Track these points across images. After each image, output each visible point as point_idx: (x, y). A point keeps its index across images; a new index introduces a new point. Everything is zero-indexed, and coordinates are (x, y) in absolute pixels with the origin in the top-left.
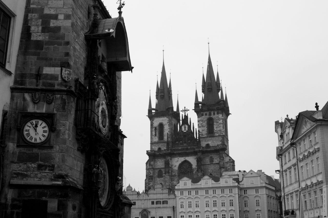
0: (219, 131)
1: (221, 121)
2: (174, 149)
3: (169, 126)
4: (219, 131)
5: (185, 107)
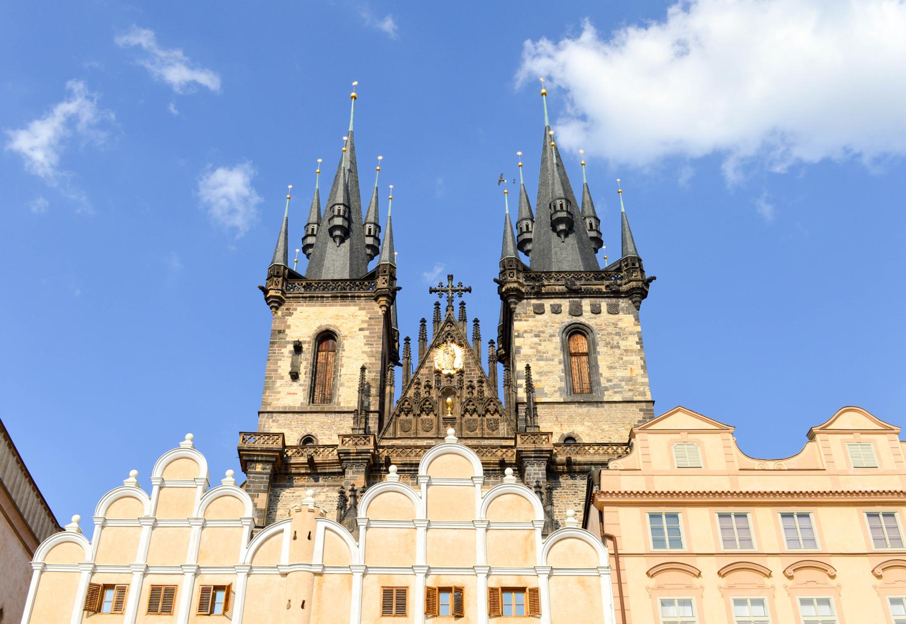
0: (623, 384)
1: (632, 342)
2: (389, 447)
3: (365, 344)
4: (623, 384)
5: (450, 278)
